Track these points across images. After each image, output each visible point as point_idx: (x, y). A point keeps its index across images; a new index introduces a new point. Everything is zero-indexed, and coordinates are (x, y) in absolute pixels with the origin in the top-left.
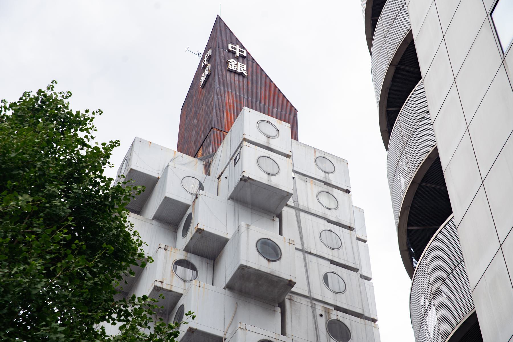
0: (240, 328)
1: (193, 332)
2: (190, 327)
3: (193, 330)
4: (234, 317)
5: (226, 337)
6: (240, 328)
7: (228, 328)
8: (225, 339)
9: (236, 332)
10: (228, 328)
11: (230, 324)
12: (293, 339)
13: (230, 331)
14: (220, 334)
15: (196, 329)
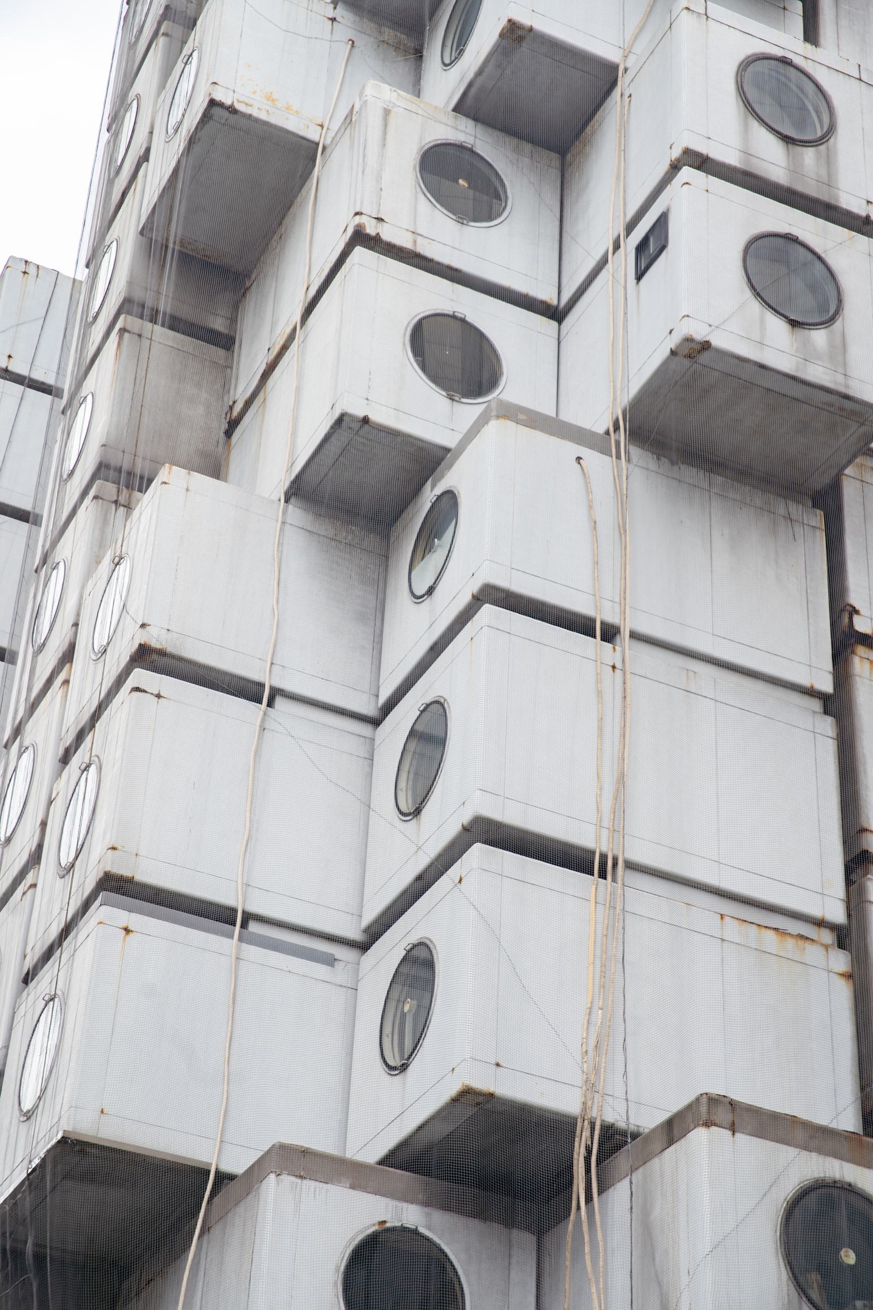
0: (687, 8)
1: (520, 39)
2: (510, 21)
3: (520, 33)
4: (652, 7)
5: (629, 64)
6: (687, 8)
7: (636, 37)
8: (626, 70)
9: (670, 27)
10: (636, 37)
11: (641, 29)
12: (859, 65)
13: (638, 49)
14: (609, 53)
15: (531, 29)
